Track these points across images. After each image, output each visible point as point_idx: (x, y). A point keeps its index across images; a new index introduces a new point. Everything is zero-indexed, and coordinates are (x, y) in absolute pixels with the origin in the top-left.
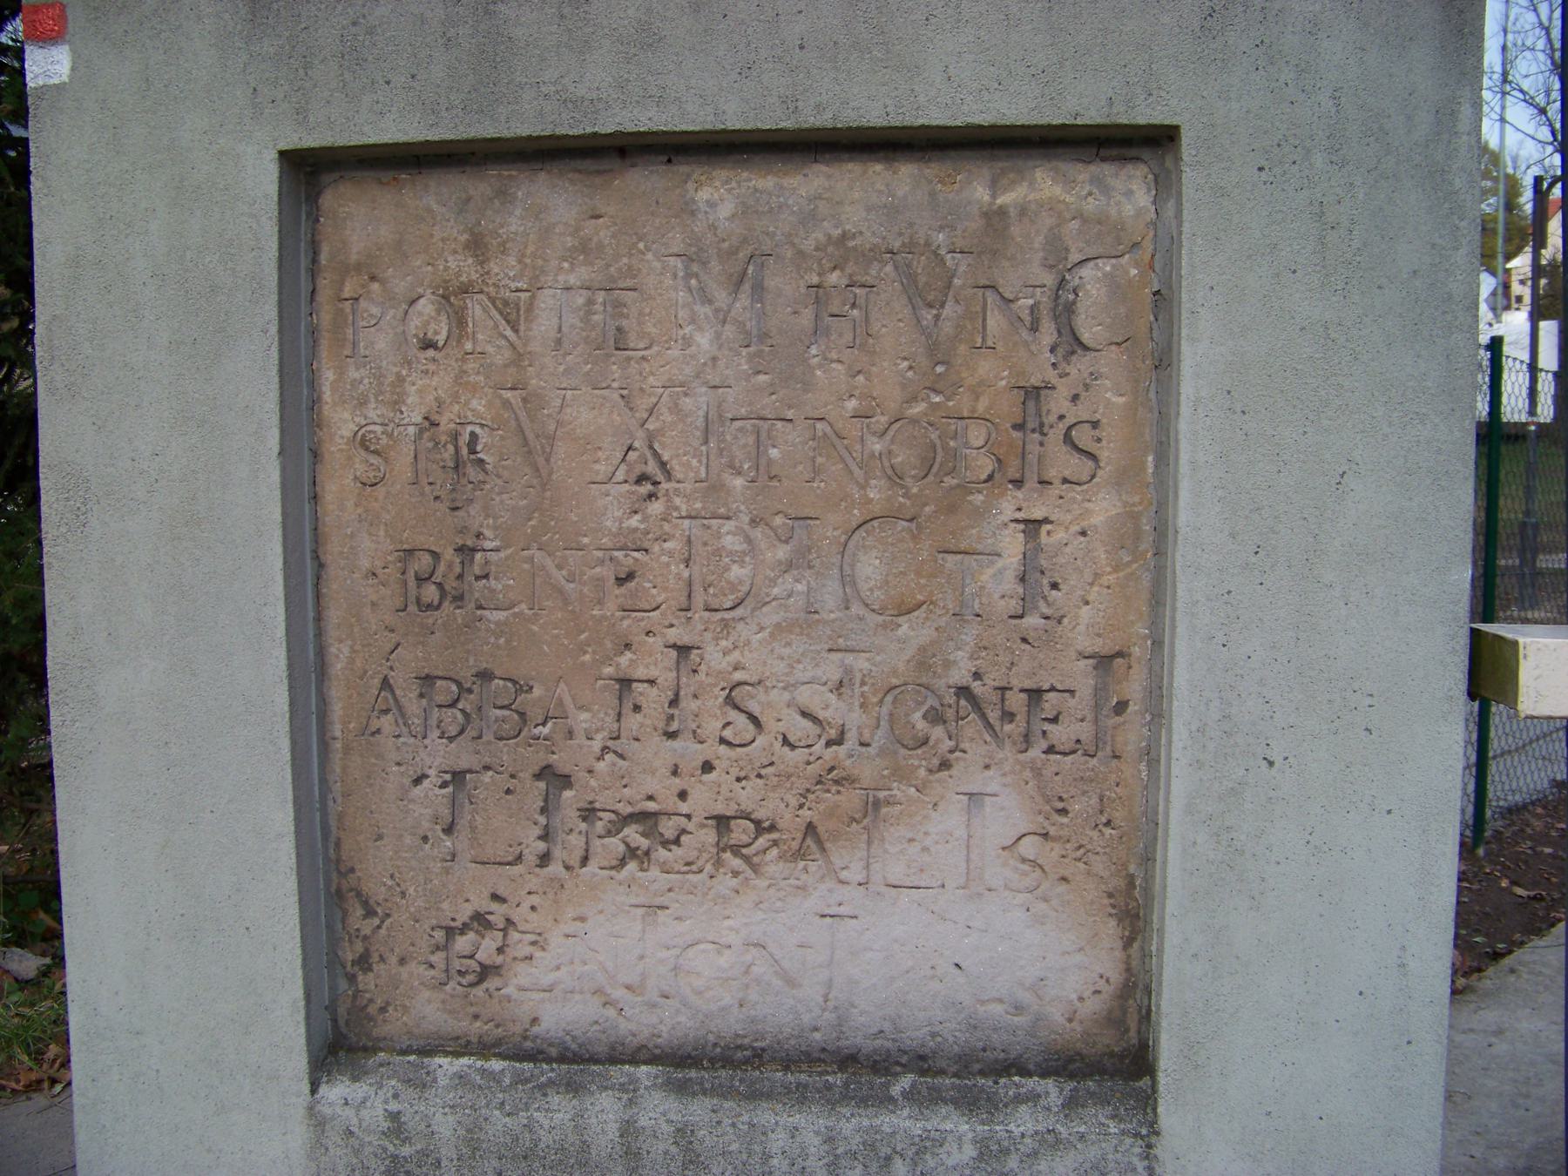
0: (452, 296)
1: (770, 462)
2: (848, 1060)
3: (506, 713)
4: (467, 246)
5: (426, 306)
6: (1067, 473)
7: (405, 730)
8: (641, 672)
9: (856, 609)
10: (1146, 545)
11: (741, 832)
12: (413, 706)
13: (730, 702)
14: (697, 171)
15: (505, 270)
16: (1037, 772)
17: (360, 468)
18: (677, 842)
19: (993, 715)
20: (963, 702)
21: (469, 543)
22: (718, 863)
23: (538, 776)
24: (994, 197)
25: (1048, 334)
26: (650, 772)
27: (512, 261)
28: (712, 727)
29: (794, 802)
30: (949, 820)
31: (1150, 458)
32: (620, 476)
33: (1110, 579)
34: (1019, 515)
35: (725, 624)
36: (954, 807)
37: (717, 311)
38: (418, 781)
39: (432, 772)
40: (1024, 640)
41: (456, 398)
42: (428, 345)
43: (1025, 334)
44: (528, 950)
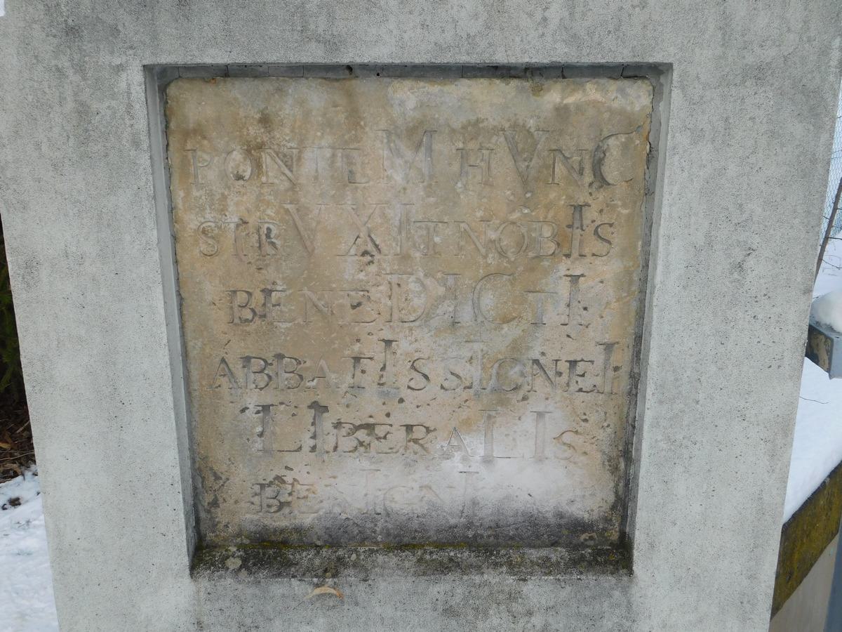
0: (253, 150)
1: (435, 245)
3: (292, 375)
5: (237, 156)
6: (594, 251)
7: (235, 385)
11: (419, 433)
13: (413, 367)
14: (396, 83)
17: (203, 247)
20: (535, 366)
21: (269, 287)
23: (310, 407)
24: (563, 99)
25: (588, 177)
26: (370, 406)
28: (404, 381)
31: (640, 243)
32: (353, 252)
34: (568, 273)
36: (528, 423)
37: (406, 162)
38: (243, 411)
39: (251, 406)
40: (568, 336)
41: (257, 208)
42: (239, 177)
43: (575, 175)
44: (305, 494)
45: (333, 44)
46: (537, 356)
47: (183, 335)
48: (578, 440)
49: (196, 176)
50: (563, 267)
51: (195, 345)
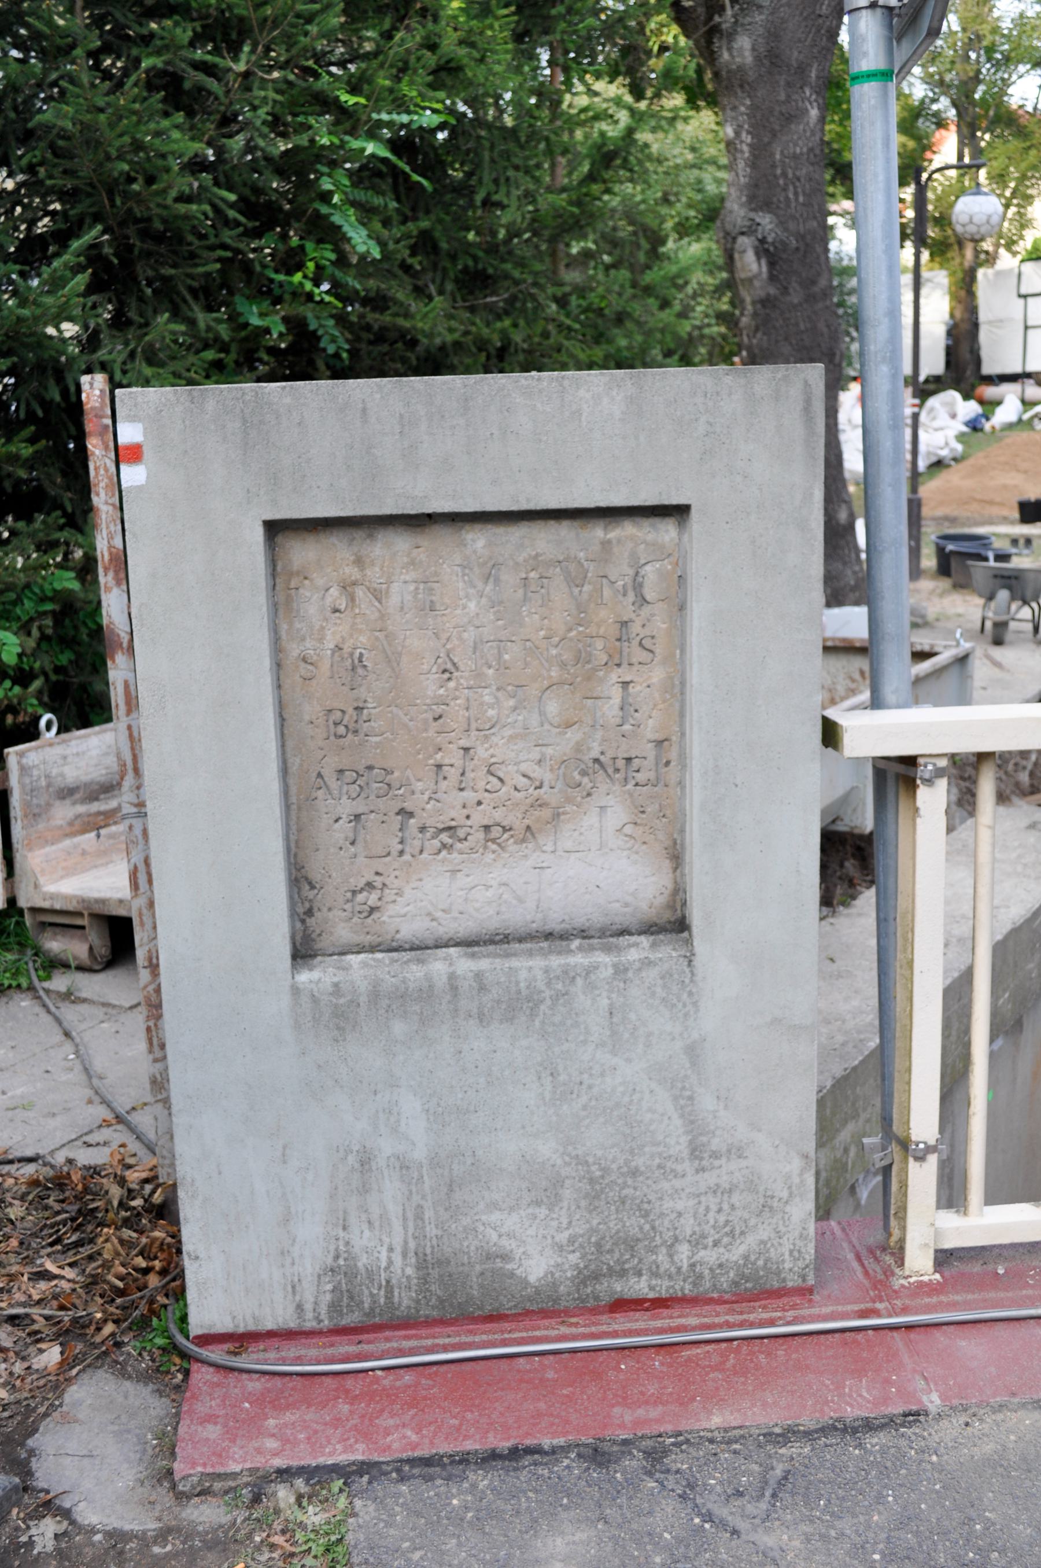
0: (347, 587)
2: (549, 936)
4: (354, 562)
5: (334, 592)
8: (447, 761)
9: (547, 726)
10: (677, 690)
11: (496, 832)
12: (334, 784)
13: (489, 772)
14: (468, 527)
15: (374, 575)
16: (631, 795)
17: (303, 672)
19: (610, 771)
22: (485, 847)
23: (398, 814)
25: (631, 596)
26: (452, 806)
27: (377, 569)
28: (481, 785)
29: (520, 816)
30: (591, 819)
32: (434, 670)
33: (661, 706)
35: (486, 737)
38: (336, 821)
41: (351, 636)
42: (336, 611)
43: (621, 598)
44: (394, 897)
48: (639, 830)
49: (298, 611)
51: (295, 763)
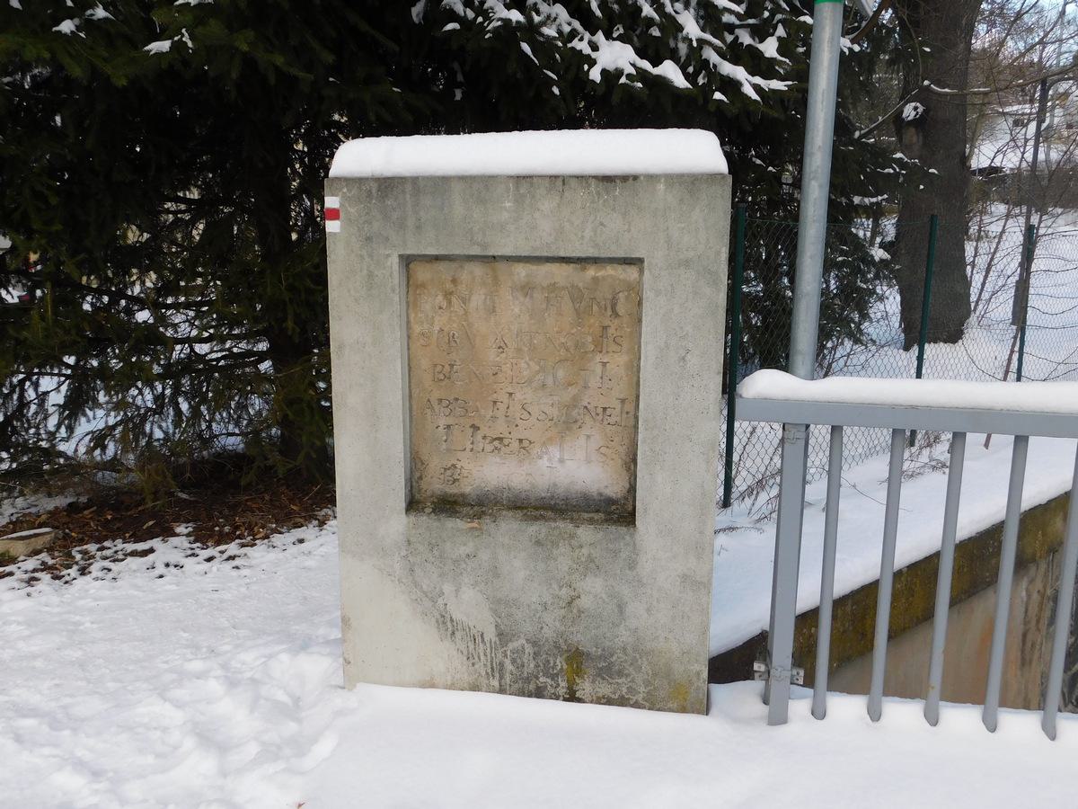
0: (448, 295)
5: (440, 298)
10: (635, 369)
11: (526, 443)
12: (436, 407)
14: (516, 265)
18: (508, 445)
26: (500, 428)
28: (518, 415)
36: (582, 440)
42: (440, 308)
45: (485, 246)
46: (585, 404)
47: (410, 386)
49: (420, 307)
50: (598, 358)
51: (415, 392)
